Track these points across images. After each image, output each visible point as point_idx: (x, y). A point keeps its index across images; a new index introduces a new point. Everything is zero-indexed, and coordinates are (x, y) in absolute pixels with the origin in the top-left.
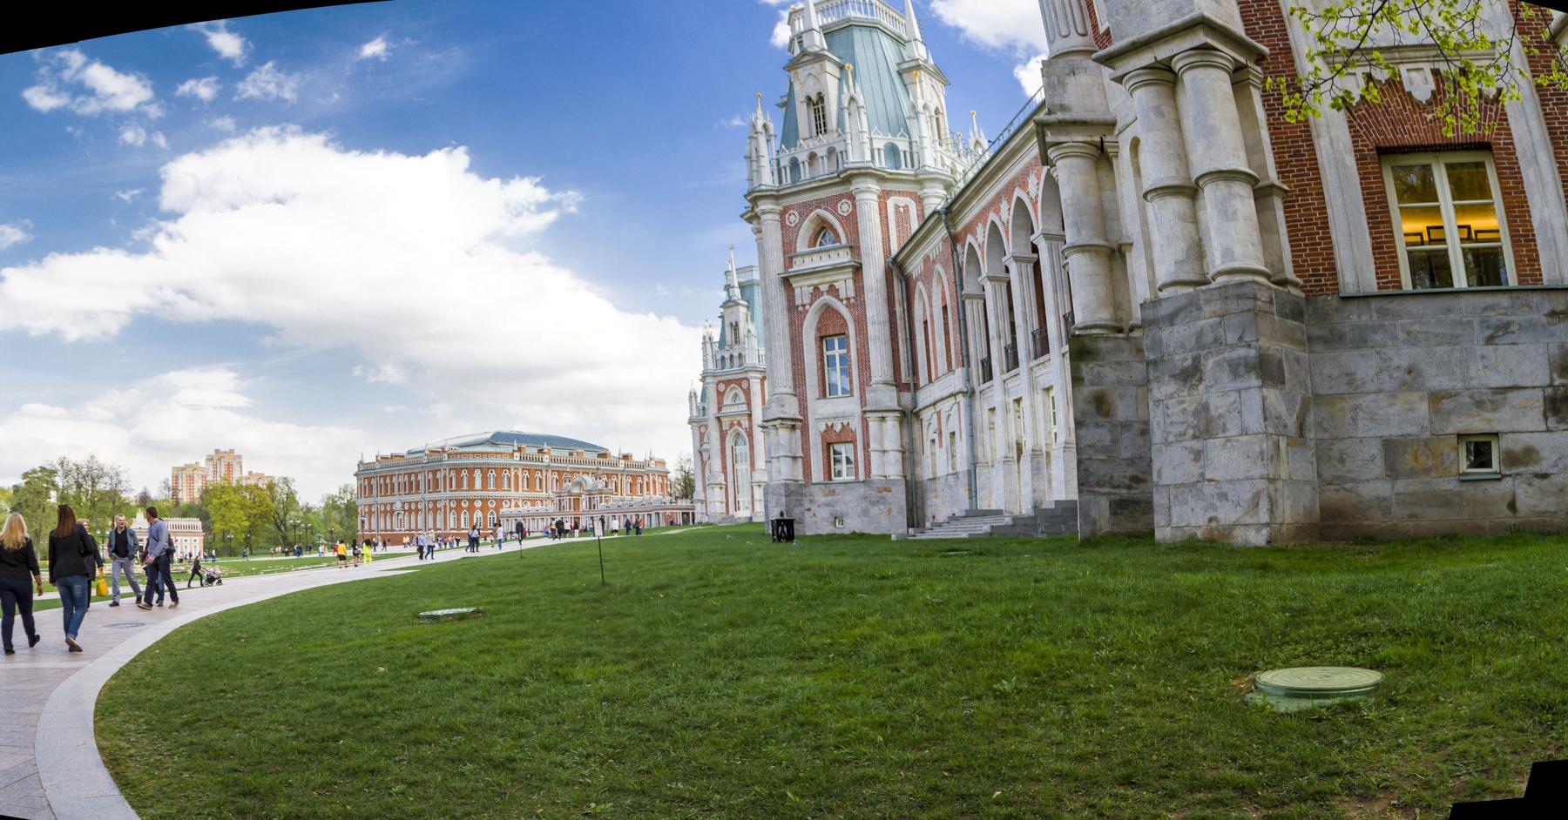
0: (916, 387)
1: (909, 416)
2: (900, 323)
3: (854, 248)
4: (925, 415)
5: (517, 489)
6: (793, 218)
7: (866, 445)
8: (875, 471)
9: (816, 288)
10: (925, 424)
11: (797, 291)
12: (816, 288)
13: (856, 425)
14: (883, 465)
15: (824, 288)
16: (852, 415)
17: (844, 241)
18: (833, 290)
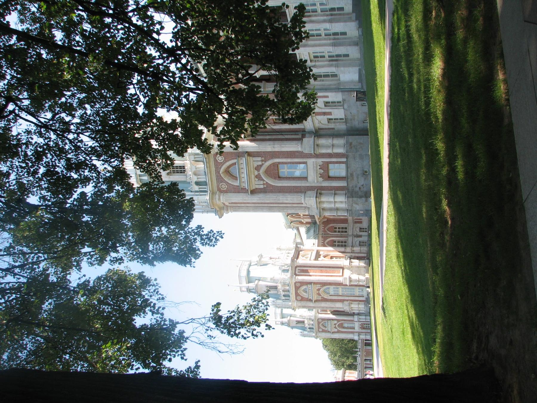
7: (330, 155)
11: (257, 187)
13: (320, 161)
14: (339, 146)
15: (256, 173)
18: (258, 168)
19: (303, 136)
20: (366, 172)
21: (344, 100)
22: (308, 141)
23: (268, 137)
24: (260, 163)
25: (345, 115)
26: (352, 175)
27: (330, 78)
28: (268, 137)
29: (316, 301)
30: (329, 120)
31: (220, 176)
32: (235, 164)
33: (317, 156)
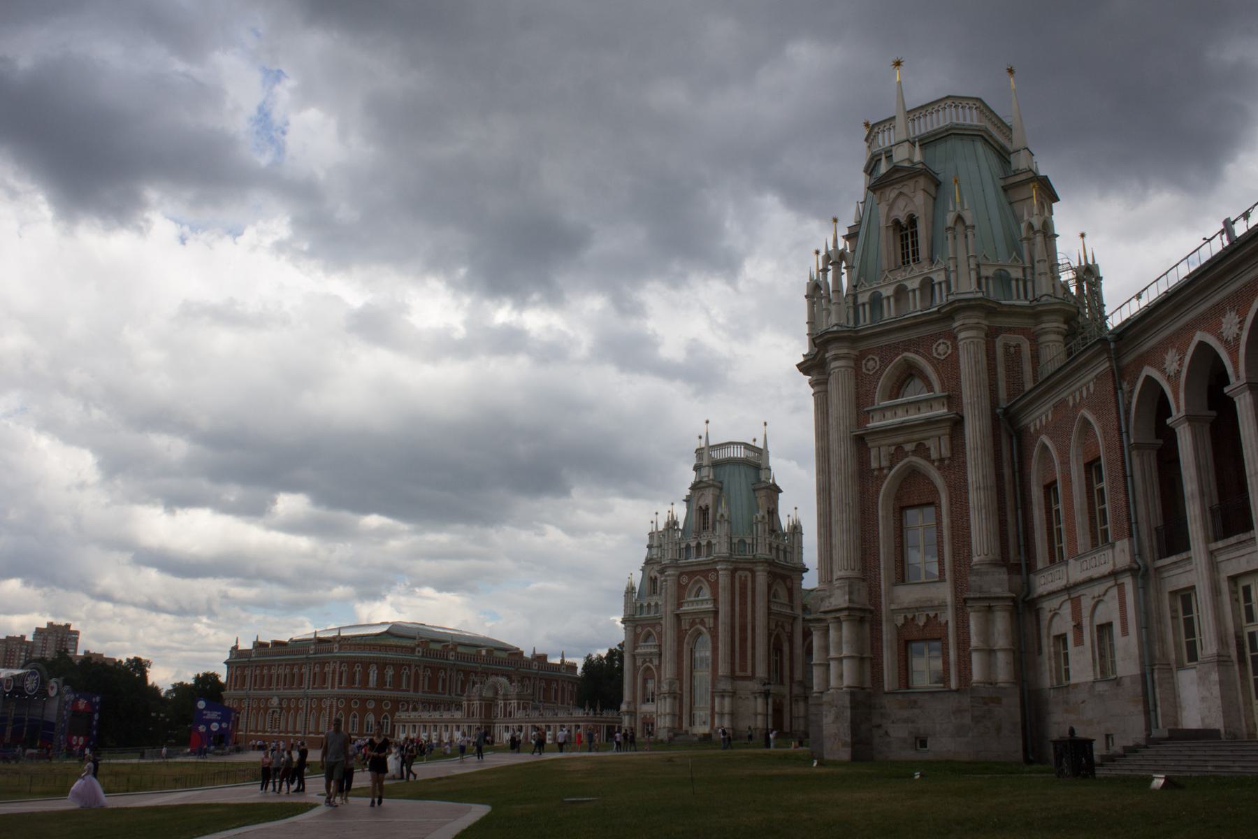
0: (1031, 568)
1: (1025, 607)
2: (1008, 488)
3: (952, 399)
4: (1048, 606)
5: (416, 690)
6: (871, 365)
8: (977, 674)
9: (899, 447)
10: (1046, 616)
11: (873, 452)
12: (899, 447)
13: (949, 616)
15: (909, 447)
16: (942, 606)
17: (938, 391)
18: (921, 450)
19: (1014, 569)
20: (923, 744)
21: (1118, 682)
22: (998, 584)
23: (1007, 471)
24: (934, 455)
25: (1076, 685)
26: (913, 705)
27: (1184, 640)
28: (1007, 471)
29: (678, 616)
30: (1062, 638)
31: (897, 355)
32: (931, 389)
33: (962, 605)
